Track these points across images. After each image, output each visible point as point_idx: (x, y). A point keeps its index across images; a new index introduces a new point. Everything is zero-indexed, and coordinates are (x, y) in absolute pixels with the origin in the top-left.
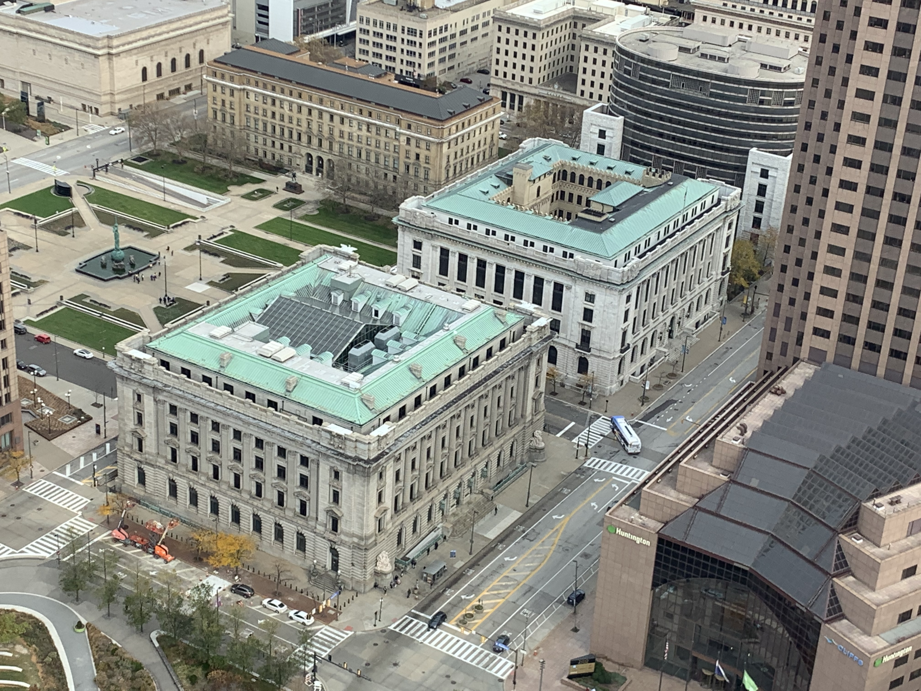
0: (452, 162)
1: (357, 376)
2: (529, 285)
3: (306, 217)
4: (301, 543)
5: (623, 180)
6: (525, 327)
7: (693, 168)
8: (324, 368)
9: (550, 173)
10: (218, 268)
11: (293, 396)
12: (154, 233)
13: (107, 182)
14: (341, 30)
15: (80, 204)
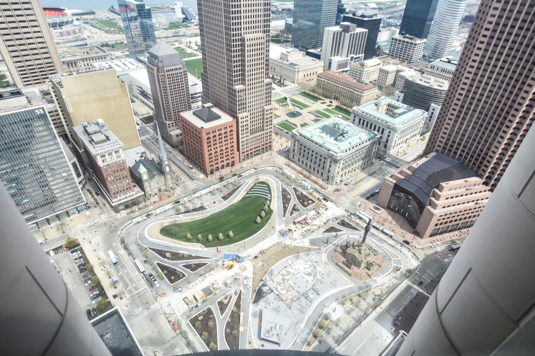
2: (377, 128)
4: (322, 174)
8: (332, 140)
10: (313, 117)
11: (325, 145)
12: (301, 109)
13: (295, 98)
14: (346, 69)
15: (288, 101)
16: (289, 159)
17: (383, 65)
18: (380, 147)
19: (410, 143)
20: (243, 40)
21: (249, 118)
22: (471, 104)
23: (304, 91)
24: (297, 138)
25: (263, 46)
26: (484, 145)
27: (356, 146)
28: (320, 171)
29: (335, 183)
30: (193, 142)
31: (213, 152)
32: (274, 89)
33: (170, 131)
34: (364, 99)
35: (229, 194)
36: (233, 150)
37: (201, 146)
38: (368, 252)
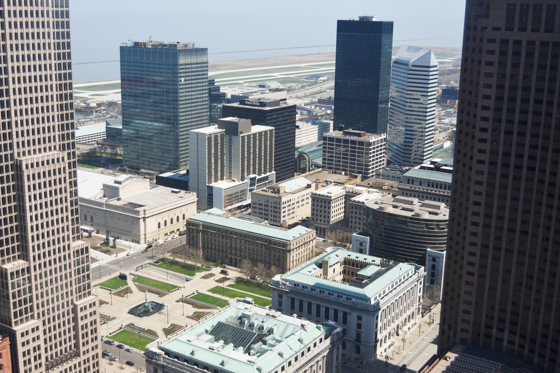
0: (295, 259)
2: (331, 313)
3: (230, 286)
5: (372, 264)
6: (331, 332)
7: (402, 258)
9: (338, 262)
14: (244, 203)
15: (130, 283)
17: (317, 188)
19: (406, 333)
20: (17, 167)
21: (40, 332)
22: (499, 239)
23: (161, 256)
24: (161, 362)
25: (63, 175)
27: (296, 359)
32: (94, 260)
34: (293, 256)
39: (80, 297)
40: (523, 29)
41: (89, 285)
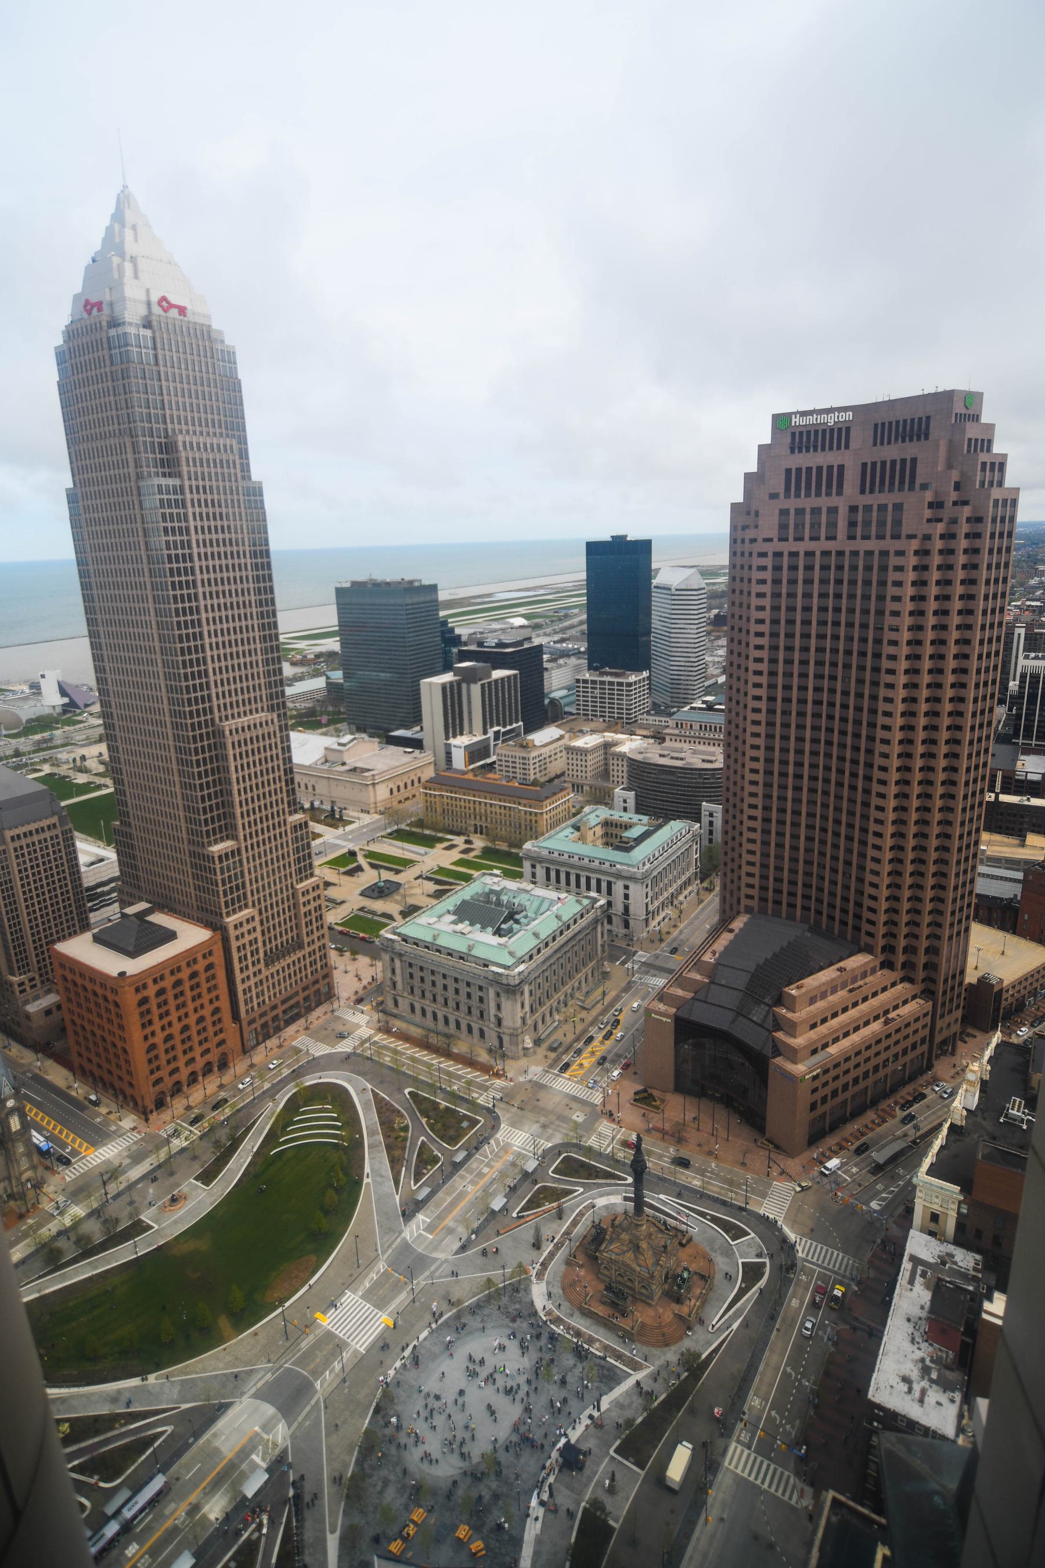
1: (505, 939)
2: (593, 883)
11: (474, 952)
12: (398, 872)
15: (362, 861)
16: (384, 1011)
18: (614, 928)
21: (256, 923)
26: (847, 875)
28: (475, 1027)
29: (521, 1053)
30: (97, 1020)
31: (160, 1037)
33: (27, 1002)
35: (217, 1159)
36: (220, 1020)
37: (121, 1027)
38: (661, 1239)
39: (301, 880)
40: (799, 539)
41: (311, 865)
